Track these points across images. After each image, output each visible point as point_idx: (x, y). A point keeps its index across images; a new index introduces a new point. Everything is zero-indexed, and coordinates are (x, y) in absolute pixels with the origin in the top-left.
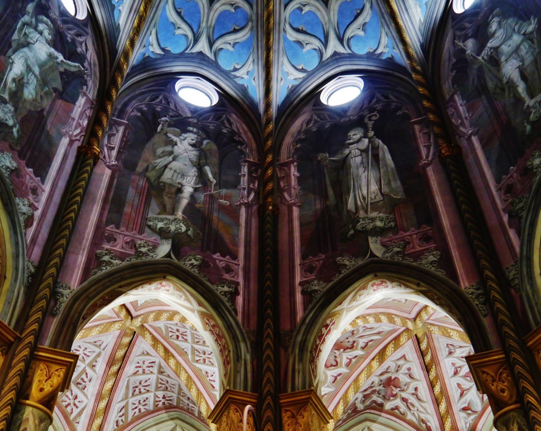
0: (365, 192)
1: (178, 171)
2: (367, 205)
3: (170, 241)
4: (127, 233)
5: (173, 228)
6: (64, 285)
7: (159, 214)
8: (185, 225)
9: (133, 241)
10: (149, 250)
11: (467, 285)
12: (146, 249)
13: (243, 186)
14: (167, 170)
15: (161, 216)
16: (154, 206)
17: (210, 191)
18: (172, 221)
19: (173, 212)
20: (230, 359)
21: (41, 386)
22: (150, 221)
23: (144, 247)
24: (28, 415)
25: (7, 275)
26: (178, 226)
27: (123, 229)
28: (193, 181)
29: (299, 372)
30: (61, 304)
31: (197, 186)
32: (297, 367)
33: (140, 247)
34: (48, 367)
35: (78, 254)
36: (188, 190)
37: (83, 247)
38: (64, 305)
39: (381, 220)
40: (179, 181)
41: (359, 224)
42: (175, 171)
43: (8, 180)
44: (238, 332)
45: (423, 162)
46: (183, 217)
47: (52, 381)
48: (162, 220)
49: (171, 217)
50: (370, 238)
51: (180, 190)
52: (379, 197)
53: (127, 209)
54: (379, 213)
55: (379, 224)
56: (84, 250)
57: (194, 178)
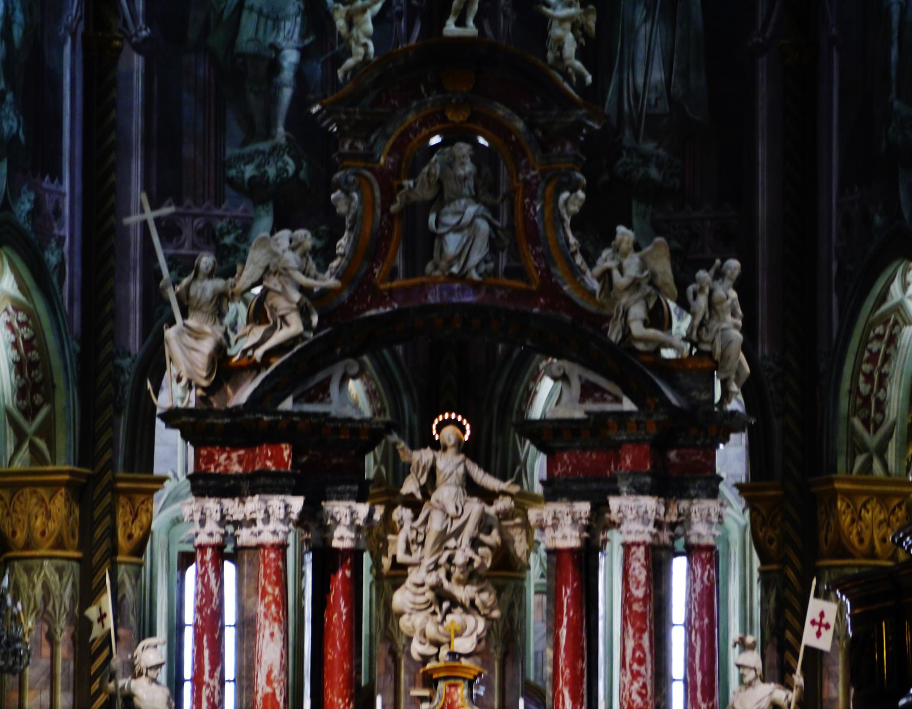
0: (640, 80)
1: (265, 10)
2: (640, 116)
3: (271, 207)
4: (196, 210)
5: (271, 171)
6: (121, 351)
7: (244, 144)
8: (292, 157)
9: (209, 226)
10: (237, 239)
11: (766, 352)
12: (232, 236)
13: (397, 8)
14: (245, 14)
15: (248, 149)
16: (234, 129)
17: (333, 47)
18: (271, 153)
19: (268, 134)
20: (380, 394)
21: (128, 531)
22: (230, 167)
23: (229, 233)
24: (123, 575)
25: (56, 381)
26: (280, 164)
27: (188, 202)
28: (296, 37)
29: (497, 450)
30: (123, 387)
31: (307, 42)
32: (494, 440)
33: (222, 235)
34: (131, 500)
35: (128, 281)
36: (291, 57)
37: (132, 265)
38: (128, 388)
39: (660, 166)
40: (270, 40)
41: (620, 162)
42: (260, 13)
43: (33, 236)
44: (397, 375)
45: (755, 40)
46: (288, 139)
47: (141, 521)
48: (249, 159)
49: (265, 146)
50: (634, 204)
51: (275, 66)
52: (663, 107)
53: (188, 152)
54: (658, 147)
55: (654, 173)
56: (135, 271)
57: (299, 19)
